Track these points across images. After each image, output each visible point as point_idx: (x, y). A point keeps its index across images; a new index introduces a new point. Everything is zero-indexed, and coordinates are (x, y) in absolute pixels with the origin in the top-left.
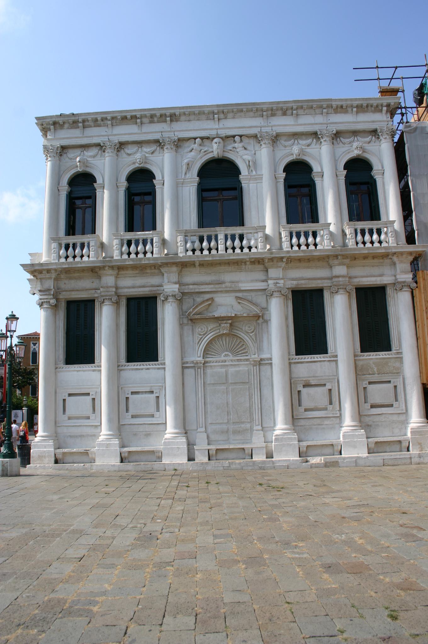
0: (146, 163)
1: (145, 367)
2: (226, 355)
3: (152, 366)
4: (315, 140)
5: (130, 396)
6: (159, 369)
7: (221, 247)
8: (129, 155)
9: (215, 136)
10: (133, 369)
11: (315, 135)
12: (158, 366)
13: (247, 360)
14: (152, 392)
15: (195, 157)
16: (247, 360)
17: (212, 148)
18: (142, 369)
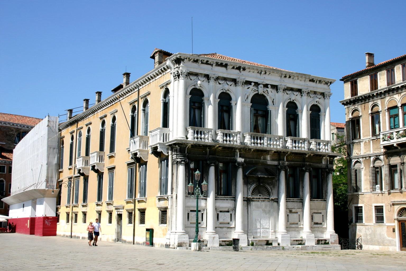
0: (228, 90)
1: (226, 199)
2: (260, 196)
3: (229, 199)
4: (299, 93)
5: (219, 213)
6: (232, 200)
7: (265, 144)
8: (220, 84)
9: (261, 83)
10: (220, 199)
11: (300, 91)
12: (232, 199)
13: (268, 199)
14: (228, 212)
15: (251, 91)
16: (268, 199)
17: (258, 88)
18: (224, 200)
